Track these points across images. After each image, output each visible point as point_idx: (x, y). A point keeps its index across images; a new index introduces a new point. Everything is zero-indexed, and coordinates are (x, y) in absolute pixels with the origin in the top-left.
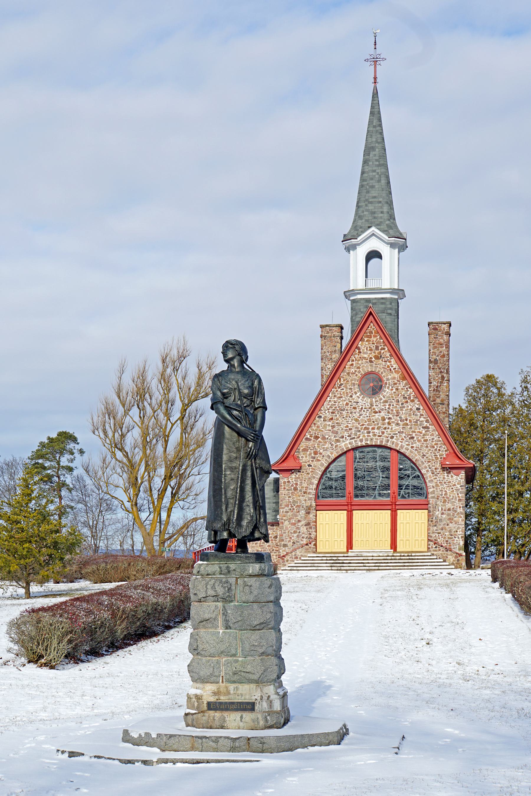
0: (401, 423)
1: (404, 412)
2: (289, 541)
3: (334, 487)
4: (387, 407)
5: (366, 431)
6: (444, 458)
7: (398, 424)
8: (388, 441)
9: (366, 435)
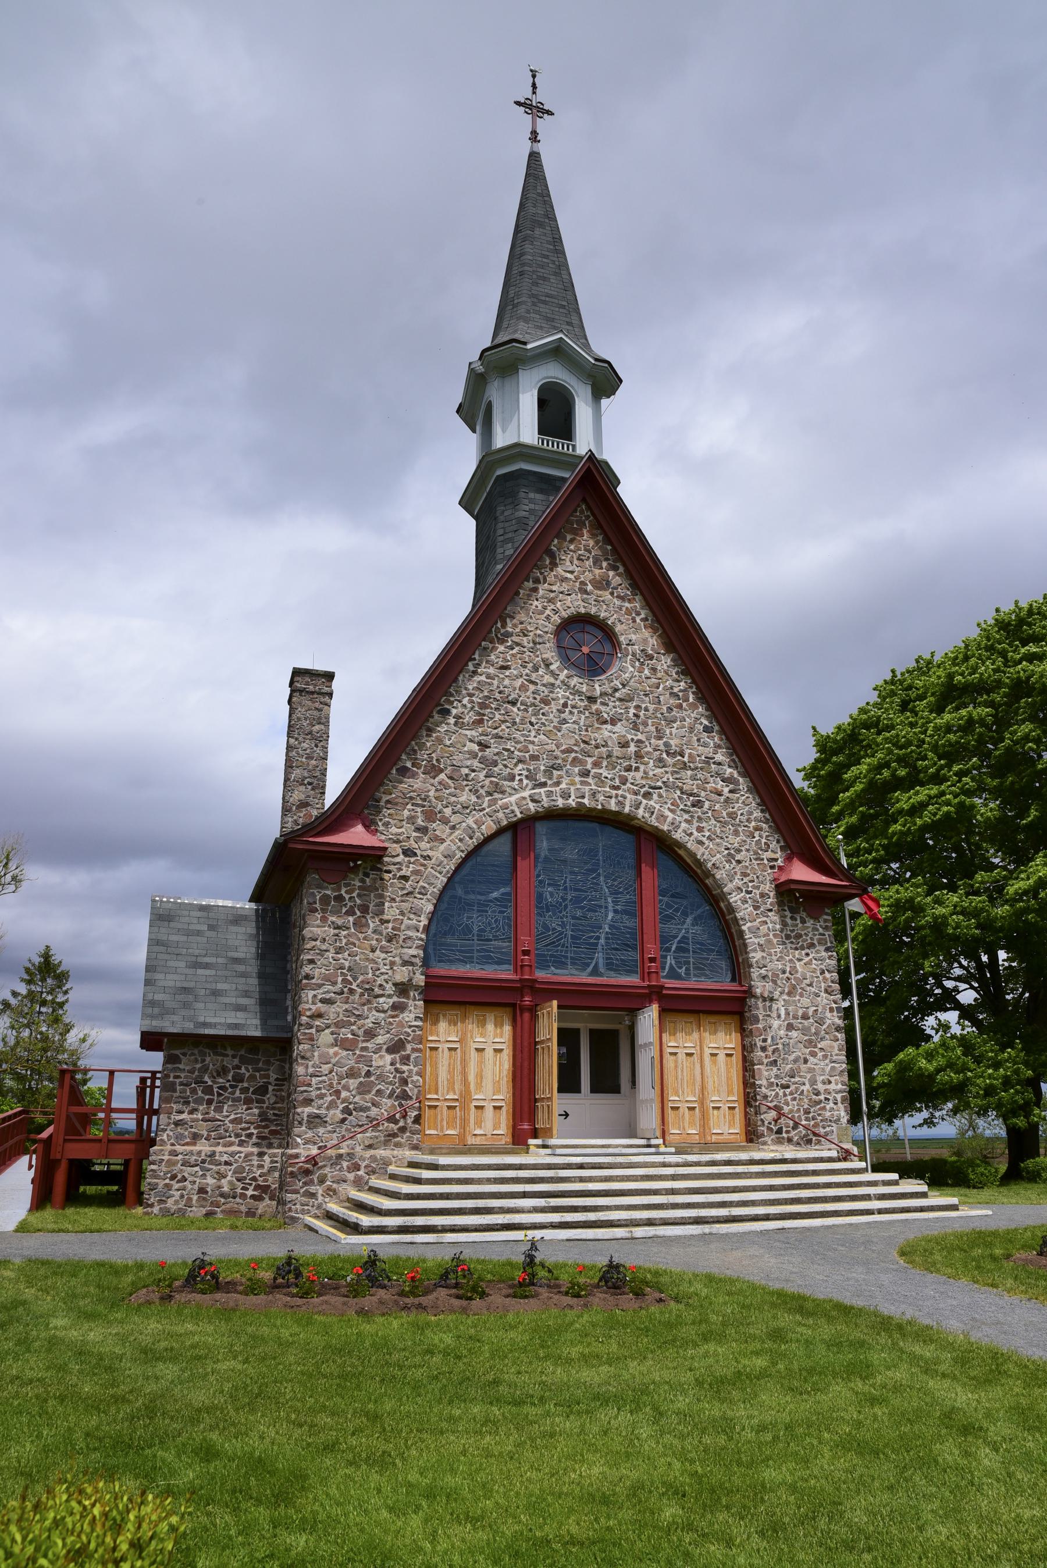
0: (670, 761)
1: (674, 731)
2: (332, 1105)
3: (475, 932)
4: (632, 711)
5: (576, 770)
6: (780, 868)
8: (638, 806)
9: (578, 779)
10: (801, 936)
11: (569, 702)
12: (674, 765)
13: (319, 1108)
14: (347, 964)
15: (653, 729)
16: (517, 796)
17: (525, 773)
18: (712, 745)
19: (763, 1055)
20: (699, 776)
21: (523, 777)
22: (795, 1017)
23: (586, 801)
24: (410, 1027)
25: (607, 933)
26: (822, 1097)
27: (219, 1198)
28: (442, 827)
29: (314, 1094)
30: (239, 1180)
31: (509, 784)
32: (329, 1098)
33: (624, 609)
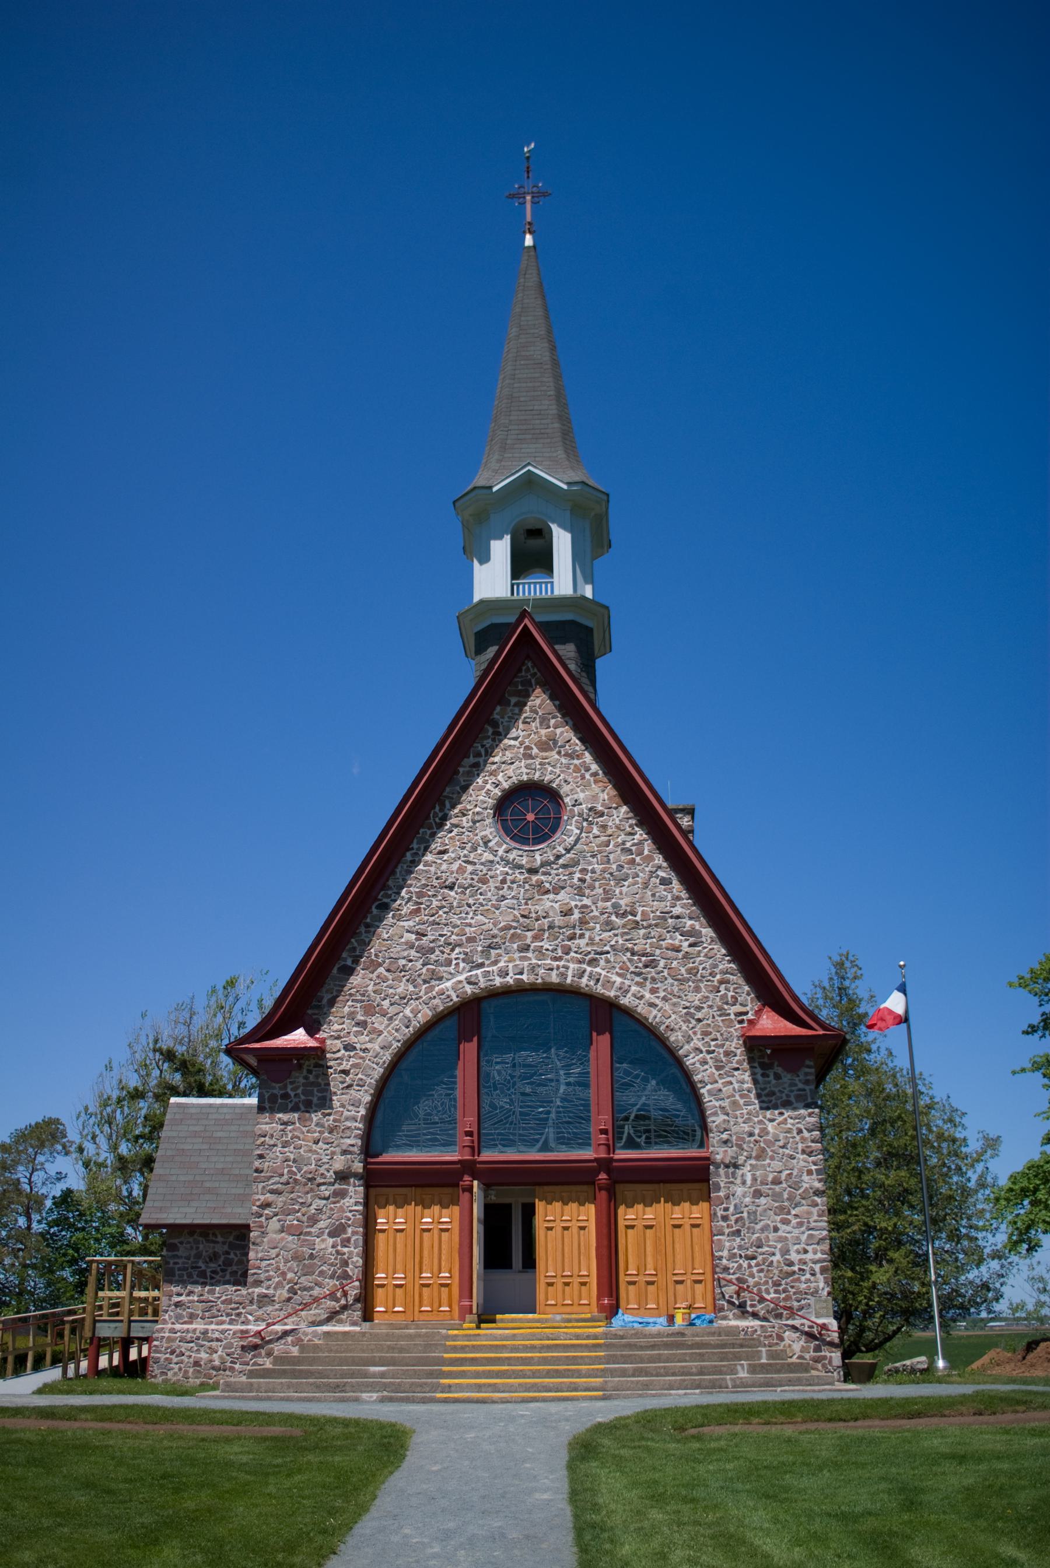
0: (619, 921)
3: (421, 1116)
4: (578, 875)
5: (515, 946)
6: (750, 1022)
7: (609, 926)
9: (517, 955)
10: (773, 1094)
11: (509, 878)
12: (624, 926)
13: (268, 1288)
14: (292, 1157)
15: (601, 891)
16: (454, 980)
17: (462, 956)
18: (669, 898)
19: (725, 1224)
20: (652, 934)
21: (460, 961)
22: (763, 1183)
23: (524, 977)
24: (351, 1211)
25: (558, 1107)
26: (796, 1268)
27: (211, 1371)
28: (381, 1019)
29: (262, 1277)
30: (228, 1355)
31: (446, 969)
32: (277, 1280)
33: (572, 767)
